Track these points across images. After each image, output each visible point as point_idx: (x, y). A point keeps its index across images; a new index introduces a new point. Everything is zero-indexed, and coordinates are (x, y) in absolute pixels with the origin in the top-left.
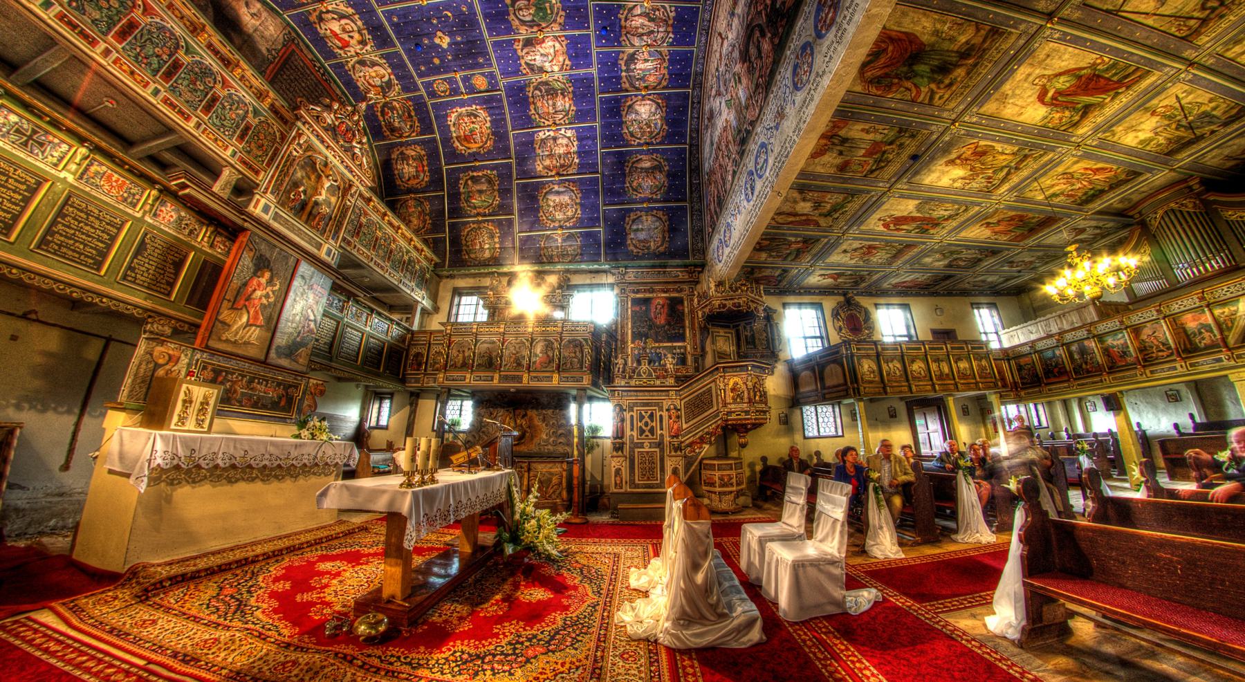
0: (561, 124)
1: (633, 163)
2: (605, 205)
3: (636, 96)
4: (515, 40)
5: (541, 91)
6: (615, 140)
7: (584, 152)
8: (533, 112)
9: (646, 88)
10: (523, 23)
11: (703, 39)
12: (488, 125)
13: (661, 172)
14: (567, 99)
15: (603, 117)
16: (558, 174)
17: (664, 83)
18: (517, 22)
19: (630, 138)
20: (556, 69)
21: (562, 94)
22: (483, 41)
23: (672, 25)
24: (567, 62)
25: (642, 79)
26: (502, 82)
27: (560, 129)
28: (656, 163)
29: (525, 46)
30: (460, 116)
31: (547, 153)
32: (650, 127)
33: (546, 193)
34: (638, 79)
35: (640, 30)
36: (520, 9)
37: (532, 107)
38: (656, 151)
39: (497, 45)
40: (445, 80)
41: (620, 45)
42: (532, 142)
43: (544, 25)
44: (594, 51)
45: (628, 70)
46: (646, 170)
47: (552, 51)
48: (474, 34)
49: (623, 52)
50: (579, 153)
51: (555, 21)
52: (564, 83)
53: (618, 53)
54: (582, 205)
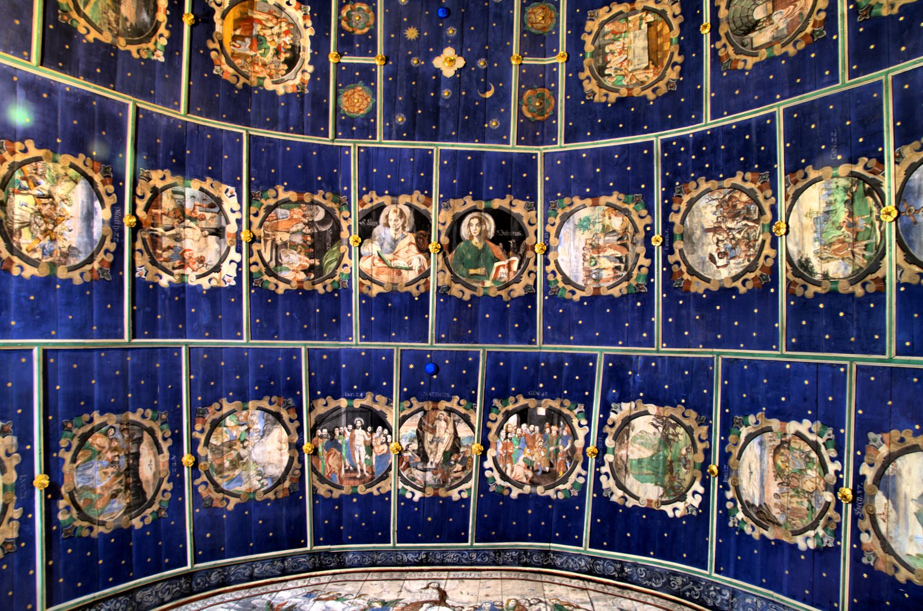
0: (250, 254)
1: (151, 432)
2: (46, 353)
3: (300, 430)
4: (429, 196)
5: (323, 222)
6: (206, 383)
7: (182, 301)
8: (283, 195)
9: (315, 452)
10: (458, 221)
11: (411, 557)
12: (269, 85)
13: (129, 509)
14: (302, 276)
15: (260, 353)
16: (137, 227)
17: (323, 490)
18: (460, 209)
19: (210, 418)
20: (366, 265)
21: (312, 268)
22: (434, 137)
23: (436, 497)
24: (376, 290)
25: (333, 443)
26: (353, 146)
27: (239, 250)
28: (150, 493)
29: (417, 213)
30: (294, 29)
31: (189, 205)
32: (234, 465)
33: (91, 181)
34: (332, 433)
35: (429, 437)
36: (481, 222)
37: (292, 195)
38: (178, 490)
39: (426, 159)
40: (373, 32)
41: (404, 397)
42: (217, 176)
43: (449, 257)
44: (397, 347)
45: (352, 413)
46: (133, 470)
47: (401, 263)
48: (450, 125)
49: (389, 403)
50: (180, 289)
51: (455, 279)
52: (332, 276)
53: (388, 393)
54: (49, 281)
